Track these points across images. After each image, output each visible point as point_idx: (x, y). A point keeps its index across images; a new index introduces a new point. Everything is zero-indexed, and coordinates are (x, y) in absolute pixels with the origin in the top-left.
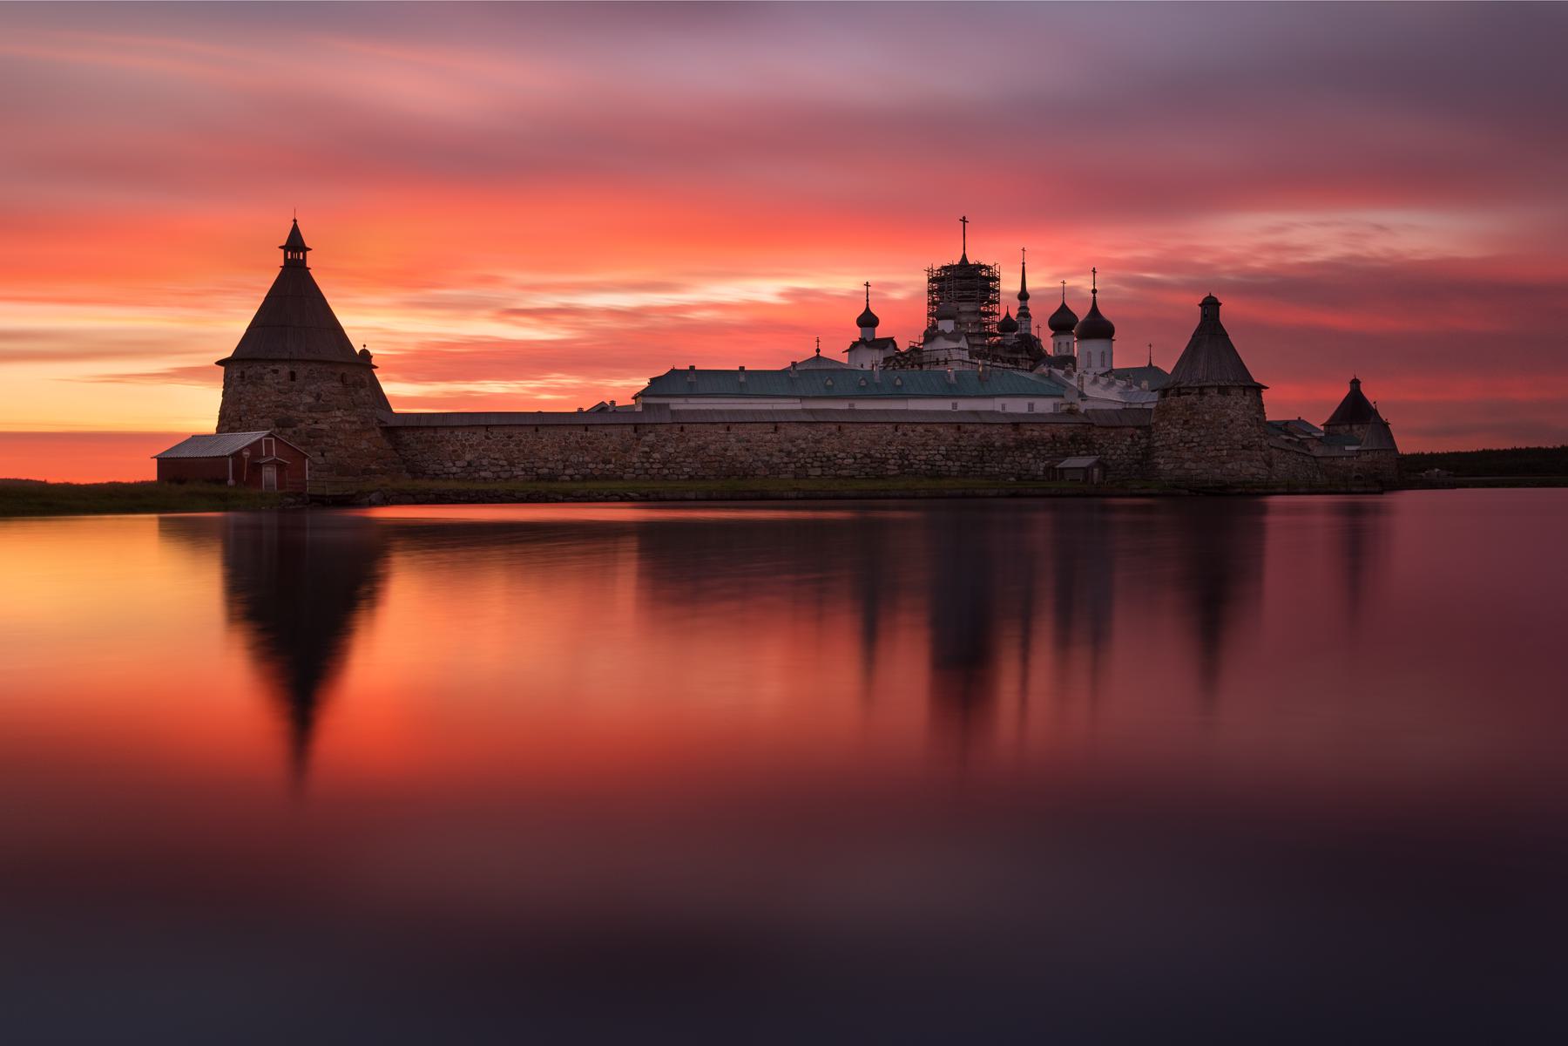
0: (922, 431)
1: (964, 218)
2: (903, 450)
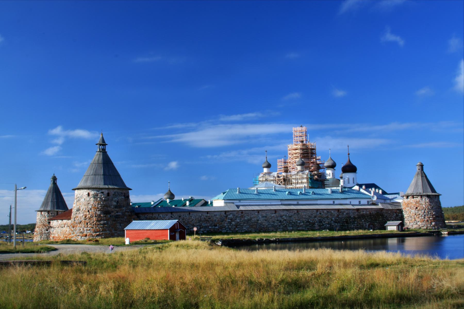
0: (326, 212)
2: (320, 219)
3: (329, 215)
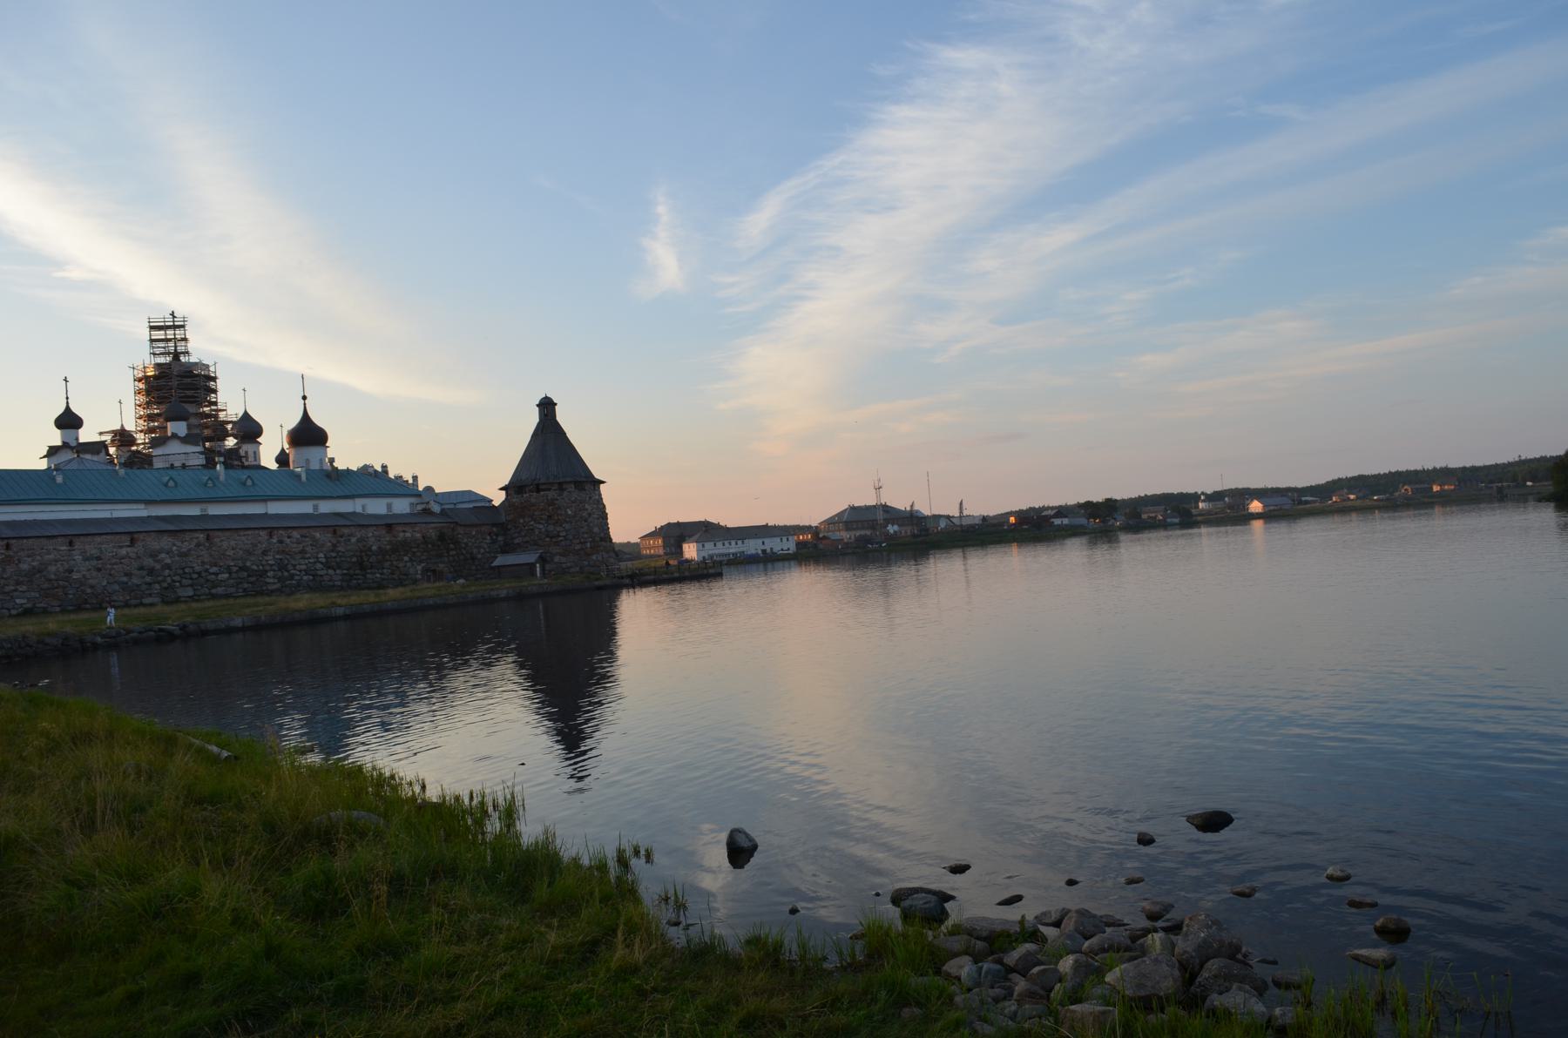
0: (299, 536)
1: (173, 312)
2: (281, 559)
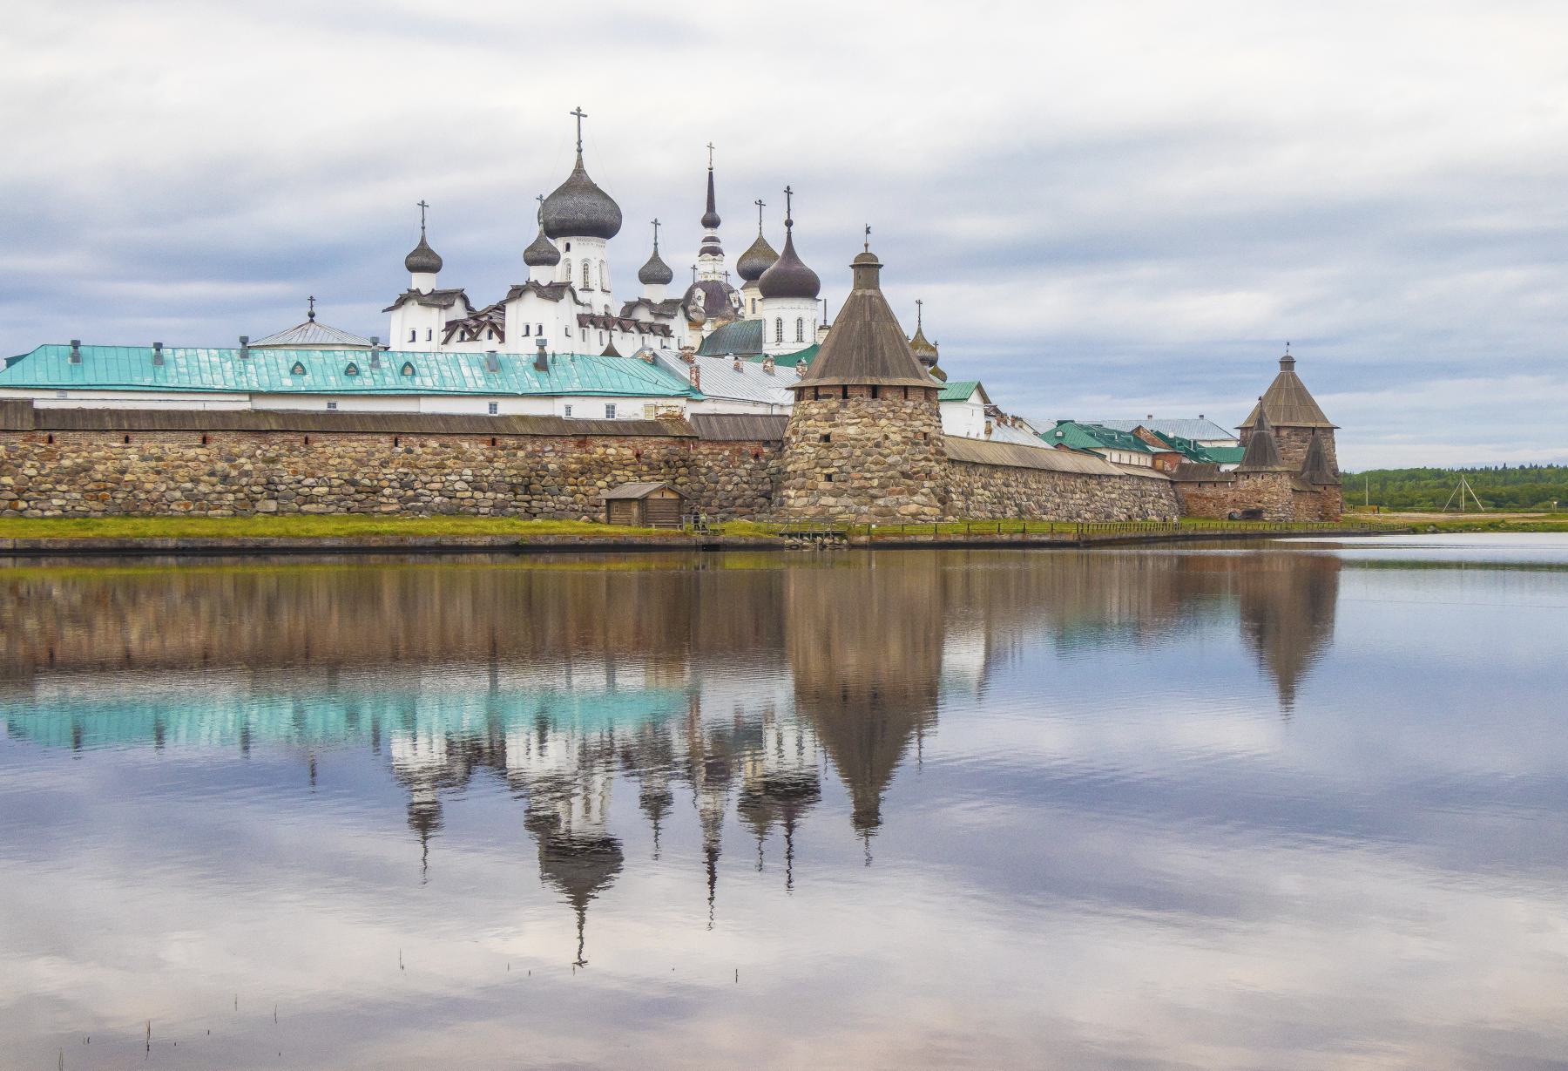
0: (436, 445)
2: (406, 474)
3: (449, 459)
